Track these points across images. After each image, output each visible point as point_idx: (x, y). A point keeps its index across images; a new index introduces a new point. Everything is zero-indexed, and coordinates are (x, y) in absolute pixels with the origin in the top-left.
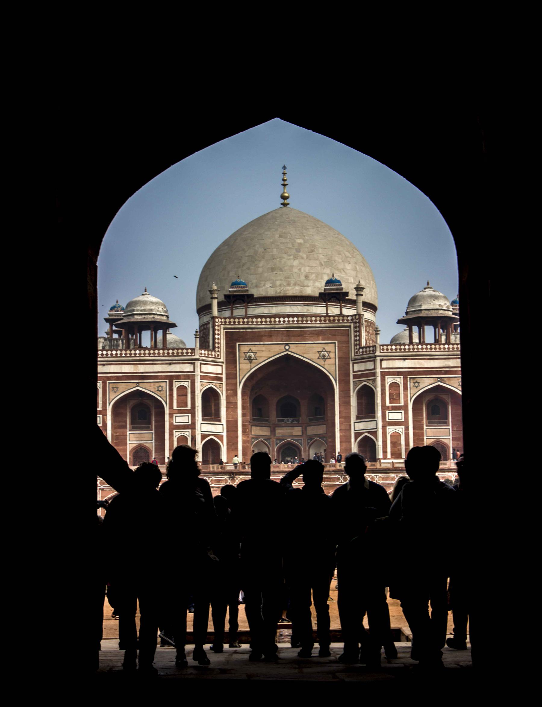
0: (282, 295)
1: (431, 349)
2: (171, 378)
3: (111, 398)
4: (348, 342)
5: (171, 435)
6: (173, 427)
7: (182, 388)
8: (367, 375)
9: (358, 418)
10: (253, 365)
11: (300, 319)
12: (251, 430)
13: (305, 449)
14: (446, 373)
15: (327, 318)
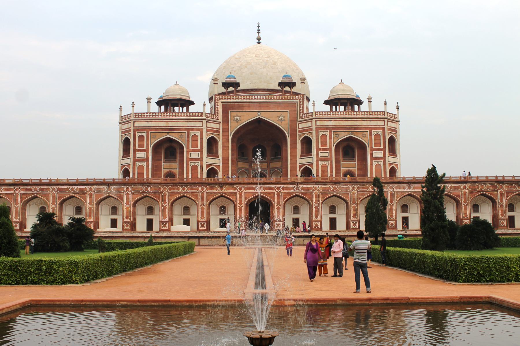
0: (256, 88)
1: (346, 114)
2: (188, 130)
3: (152, 142)
4: (295, 111)
5: (188, 164)
6: (189, 160)
7: (195, 136)
8: (307, 130)
9: (301, 156)
10: (238, 124)
11: (267, 97)
12: (237, 164)
13: (269, 176)
14: (355, 129)
15: (283, 97)
